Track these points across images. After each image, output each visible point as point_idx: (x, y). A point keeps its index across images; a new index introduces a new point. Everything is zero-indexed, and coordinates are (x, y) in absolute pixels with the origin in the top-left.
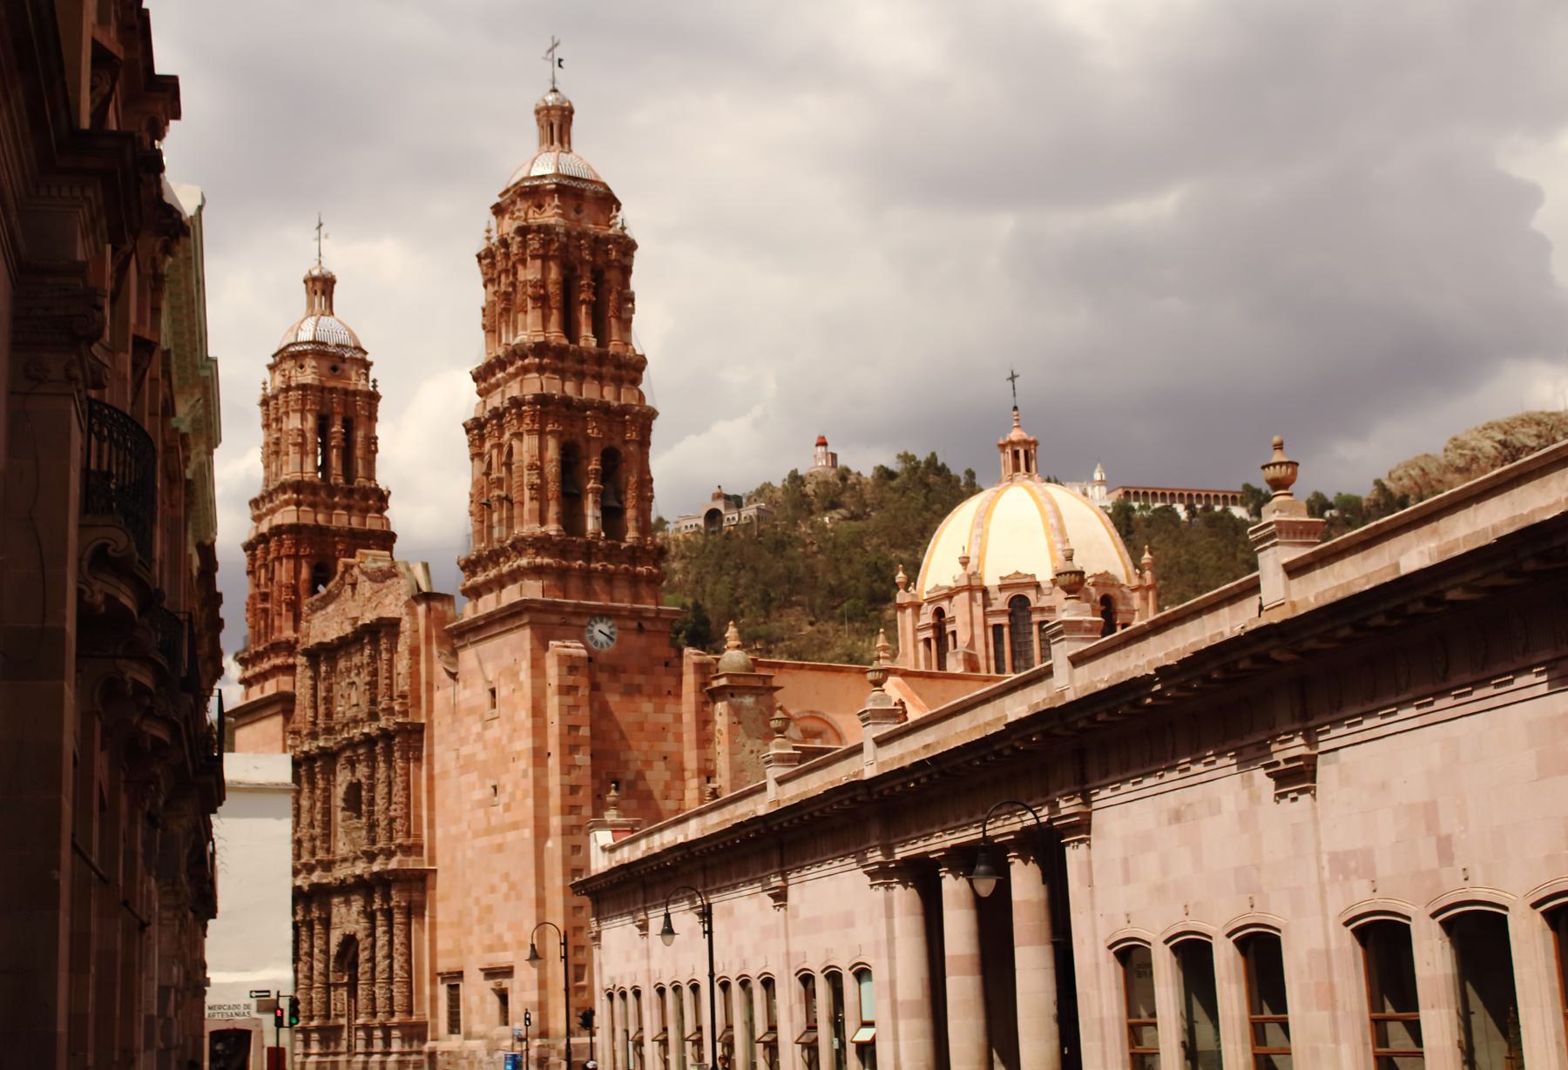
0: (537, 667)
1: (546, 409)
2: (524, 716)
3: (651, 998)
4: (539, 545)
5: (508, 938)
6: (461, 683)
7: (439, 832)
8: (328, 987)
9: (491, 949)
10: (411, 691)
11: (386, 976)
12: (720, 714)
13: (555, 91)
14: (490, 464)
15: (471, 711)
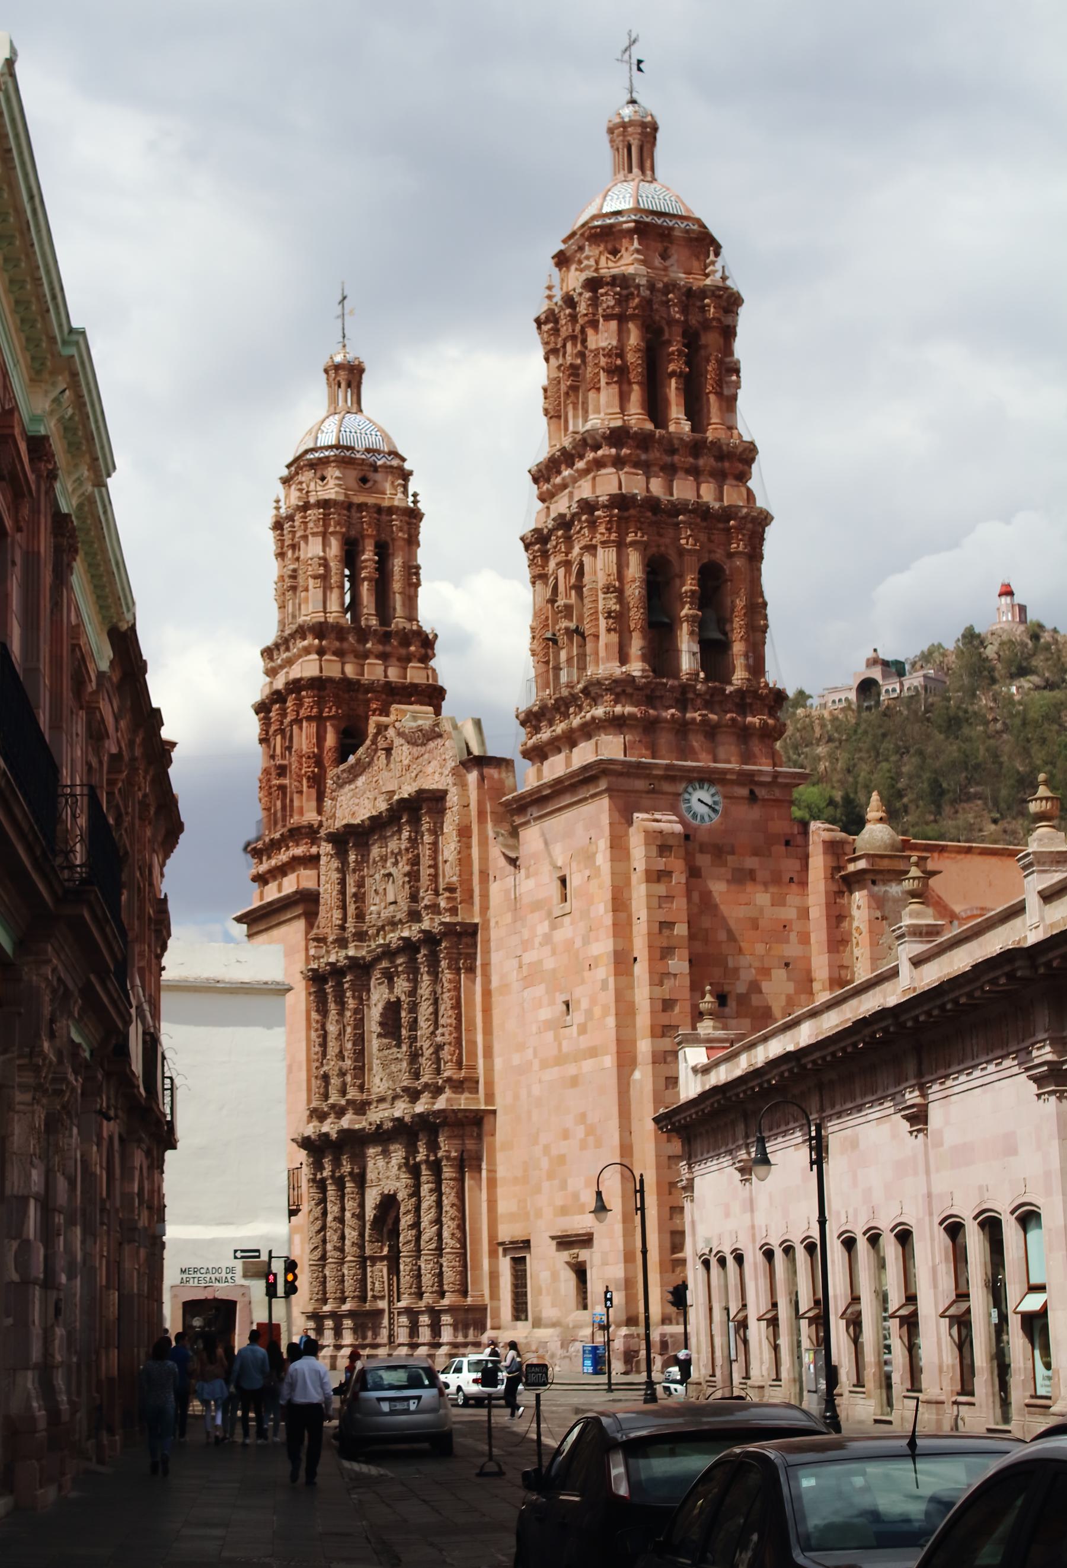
0: (618, 847)
1: (626, 514)
2: (602, 911)
3: (755, 1264)
4: (619, 690)
6: (523, 871)
7: (498, 1062)
8: (363, 1261)
9: (564, 1211)
10: (461, 882)
11: (433, 1246)
12: (859, 907)
13: (633, 102)
14: (555, 588)
15: (536, 906)
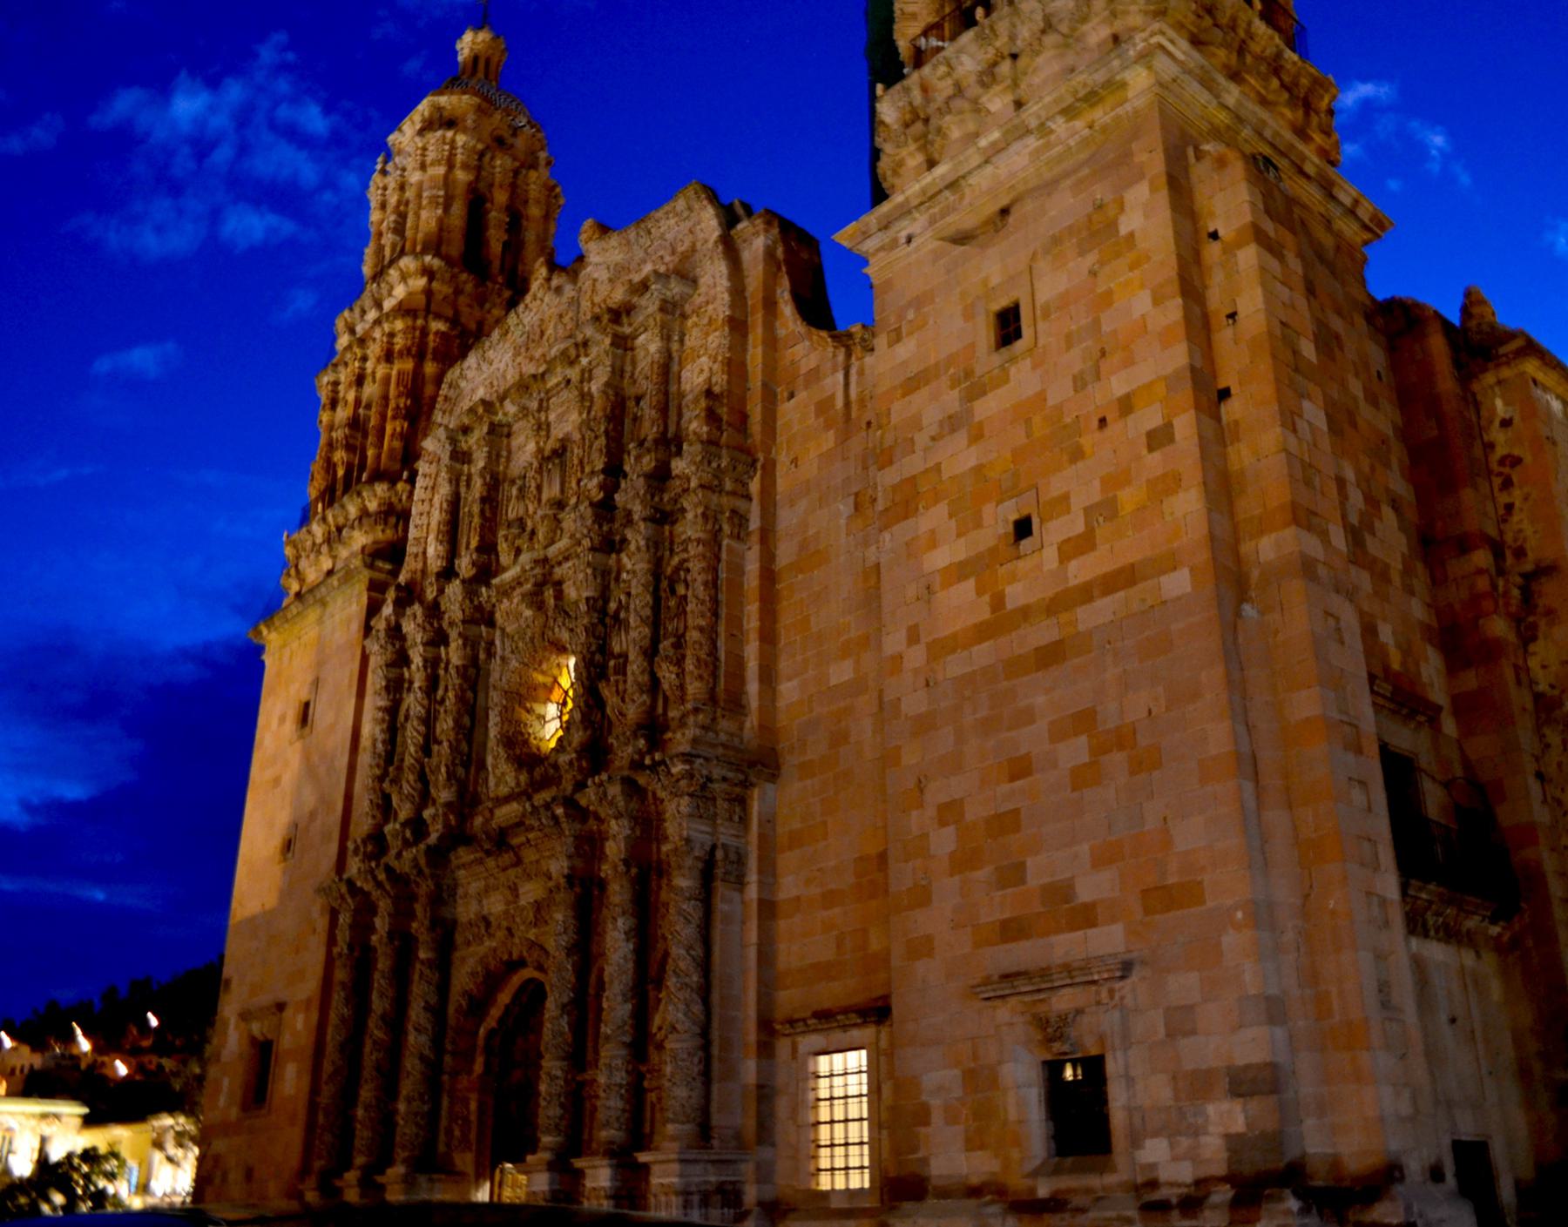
7: (788, 690)
9: (1011, 930)
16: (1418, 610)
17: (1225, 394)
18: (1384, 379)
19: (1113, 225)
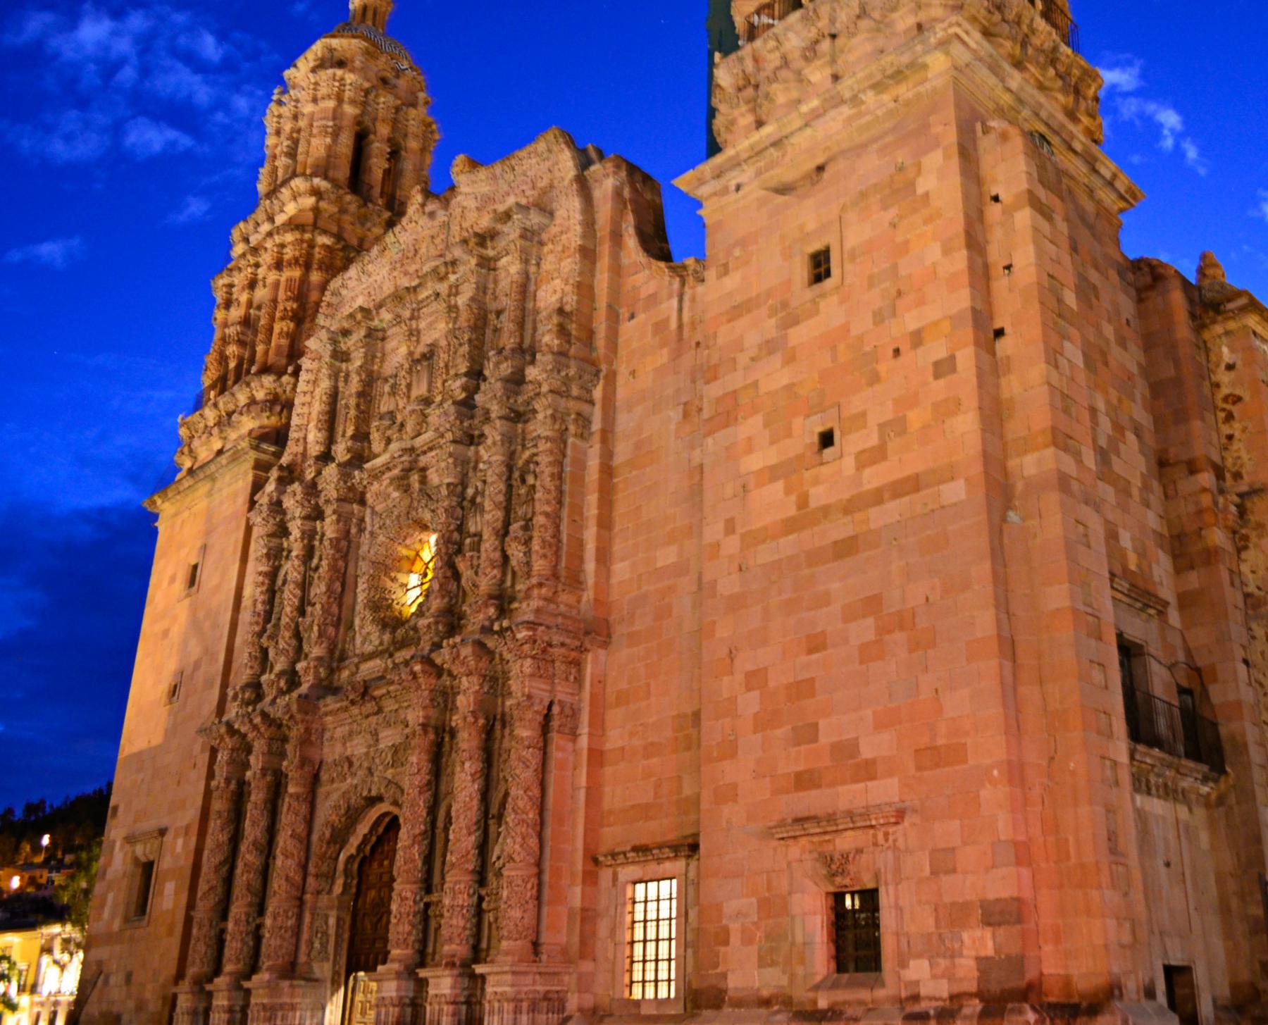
5: (872, 746)
7: (621, 570)
9: (805, 781)
16: (1152, 520)
17: (999, 333)
18: (1132, 324)
19: (911, 185)
